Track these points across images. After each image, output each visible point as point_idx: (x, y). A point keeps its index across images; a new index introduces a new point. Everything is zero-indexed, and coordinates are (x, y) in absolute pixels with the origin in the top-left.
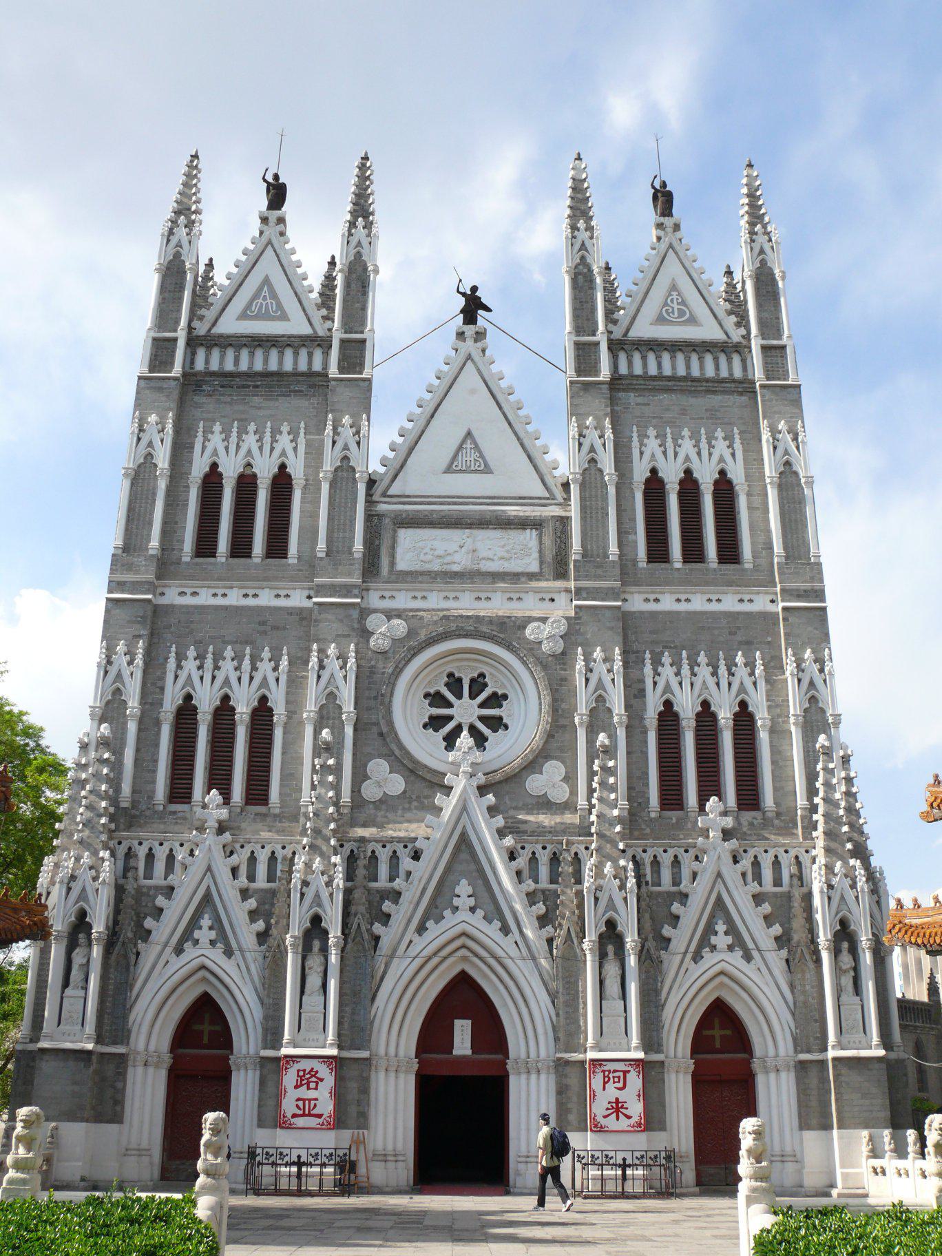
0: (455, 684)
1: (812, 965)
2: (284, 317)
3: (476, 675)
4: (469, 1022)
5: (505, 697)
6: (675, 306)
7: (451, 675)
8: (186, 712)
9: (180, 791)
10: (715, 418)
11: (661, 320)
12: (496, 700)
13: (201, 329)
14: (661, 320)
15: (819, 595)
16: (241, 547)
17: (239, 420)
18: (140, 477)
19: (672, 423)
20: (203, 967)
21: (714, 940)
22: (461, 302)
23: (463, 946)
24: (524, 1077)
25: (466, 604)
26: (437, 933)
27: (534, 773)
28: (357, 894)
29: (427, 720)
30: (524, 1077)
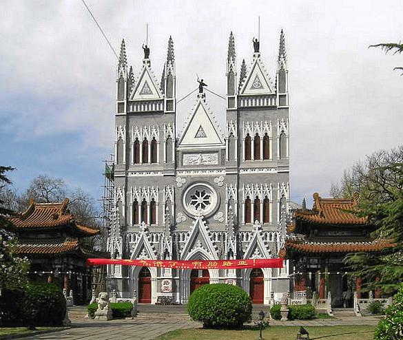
2: (151, 93)
8: (135, 203)
9: (135, 222)
10: (265, 118)
12: (207, 197)
16: (145, 161)
18: (119, 143)
19: (253, 120)
25: (200, 173)
26: (193, 251)
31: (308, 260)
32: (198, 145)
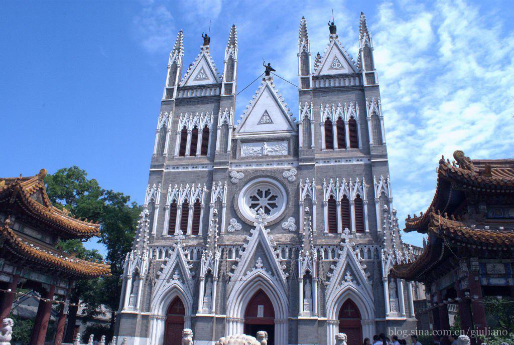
0: (267, 193)
1: (380, 287)
2: (208, 79)
3: (267, 190)
4: (263, 306)
5: (277, 197)
6: (336, 63)
7: (259, 190)
9: (172, 231)
11: (331, 68)
13: (182, 85)
14: (331, 68)
15: (385, 156)
17: (193, 112)
20: (175, 287)
21: (346, 278)
22: (265, 69)
23: (259, 280)
24: (279, 325)
25: (264, 167)
27: (285, 221)
28: (224, 263)
29: (251, 205)
30: (279, 325)
31: (483, 266)
32: (263, 132)
